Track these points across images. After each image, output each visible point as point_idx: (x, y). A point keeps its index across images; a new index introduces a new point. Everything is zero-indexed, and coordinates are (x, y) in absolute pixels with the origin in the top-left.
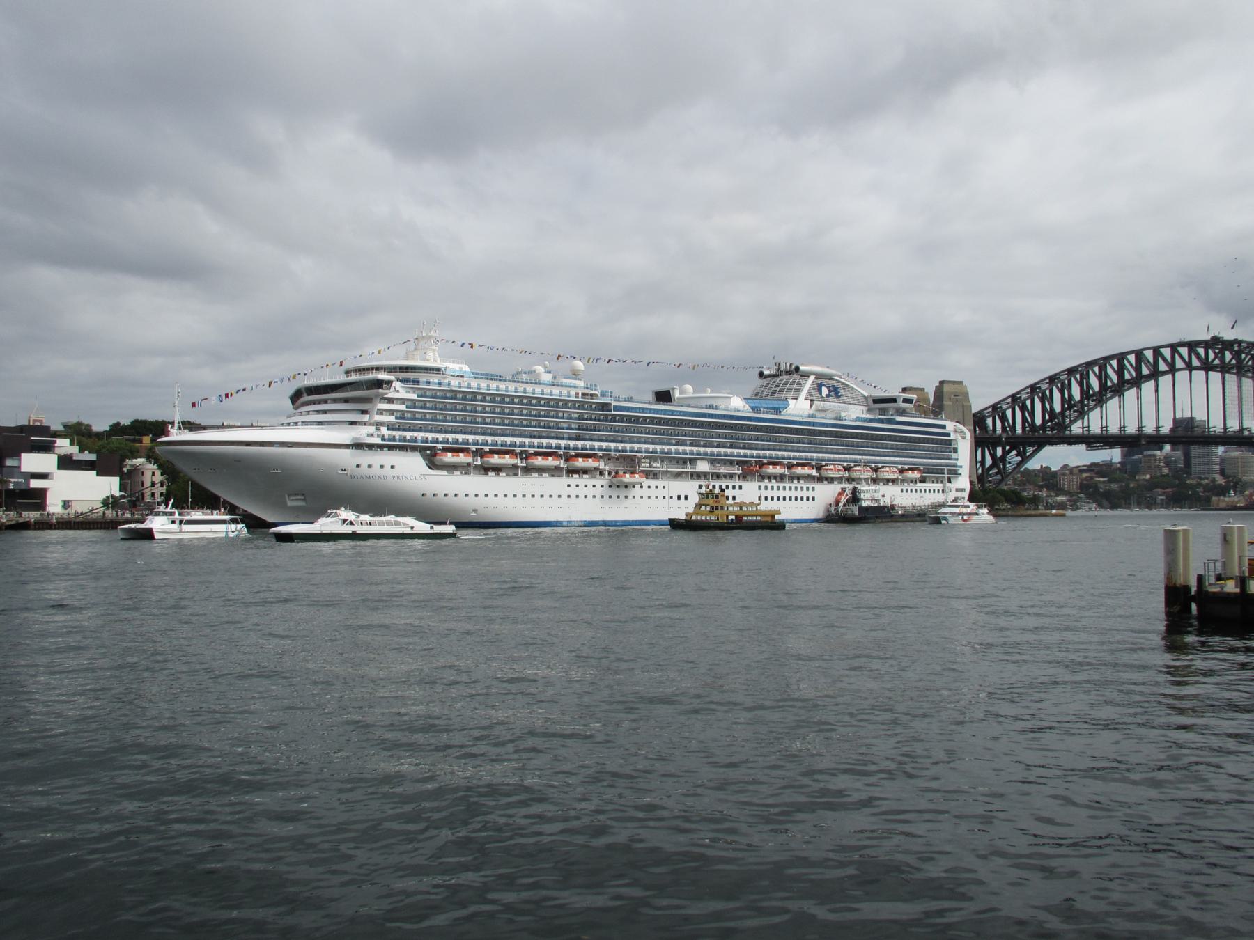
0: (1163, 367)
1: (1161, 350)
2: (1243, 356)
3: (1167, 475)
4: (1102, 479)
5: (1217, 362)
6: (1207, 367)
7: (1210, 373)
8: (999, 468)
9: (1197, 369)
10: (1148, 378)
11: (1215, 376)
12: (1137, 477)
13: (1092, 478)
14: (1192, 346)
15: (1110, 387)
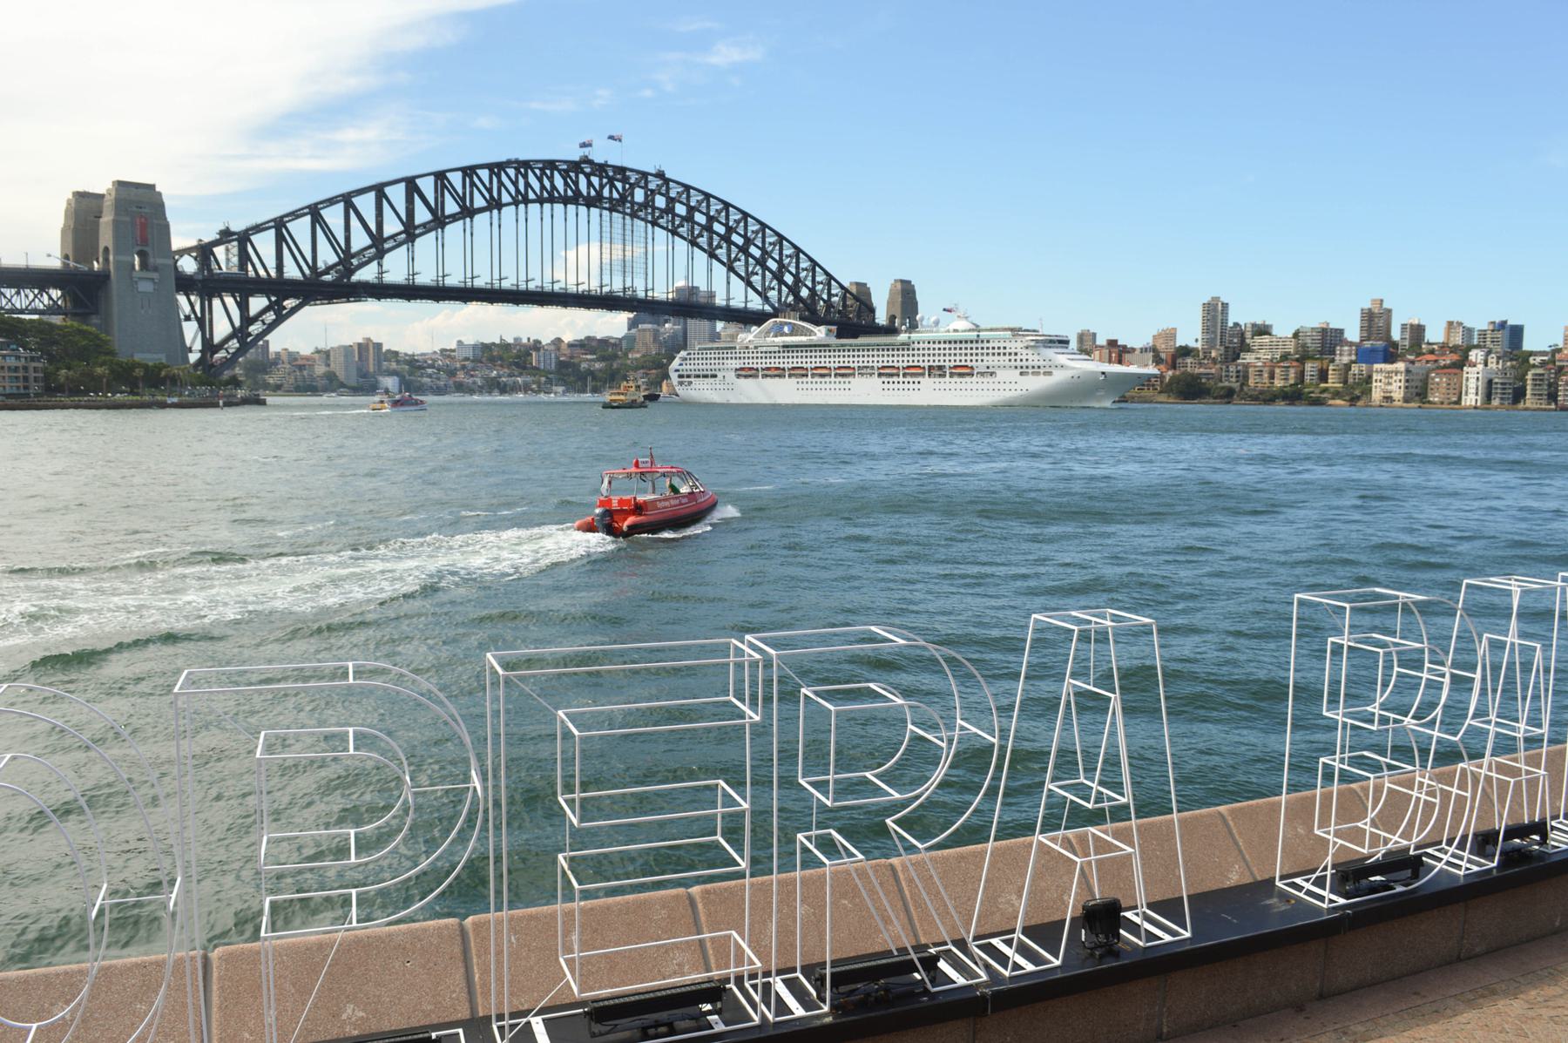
4: (589, 357)
6: (590, 203)
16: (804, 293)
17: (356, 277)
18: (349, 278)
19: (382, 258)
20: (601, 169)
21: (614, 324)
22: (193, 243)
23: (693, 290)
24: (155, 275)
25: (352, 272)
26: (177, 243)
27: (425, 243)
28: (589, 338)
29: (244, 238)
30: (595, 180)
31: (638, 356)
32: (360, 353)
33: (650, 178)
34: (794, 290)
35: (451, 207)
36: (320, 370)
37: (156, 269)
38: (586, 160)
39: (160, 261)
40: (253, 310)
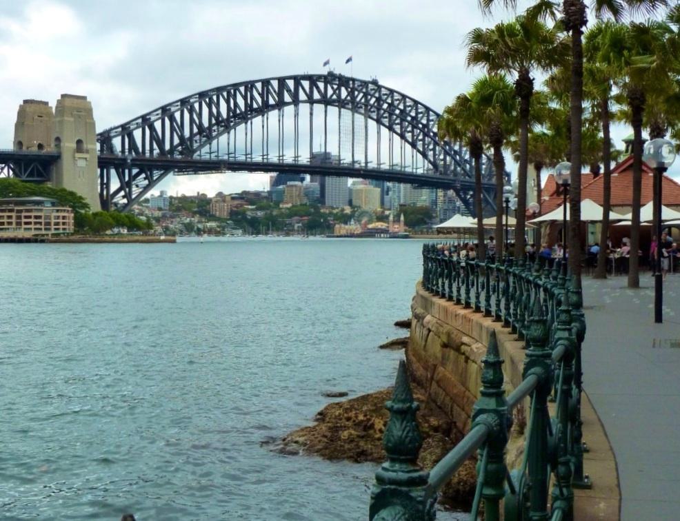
0: (287, 98)
1: (287, 81)
2: (356, 93)
3: (306, 205)
4: (250, 207)
5: (335, 97)
6: (326, 101)
7: (329, 107)
8: (125, 192)
9: (318, 102)
10: (273, 107)
11: (333, 110)
12: (281, 206)
13: (242, 205)
14: (313, 79)
15: (238, 115)
17: (196, 156)
18: (192, 157)
19: (210, 144)
21: (260, 182)
23: (326, 155)
25: (194, 151)
28: (245, 193)
29: (126, 130)
30: (335, 87)
31: (289, 205)
33: (371, 86)
37: (87, 152)
38: (331, 74)
39: (90, 146)
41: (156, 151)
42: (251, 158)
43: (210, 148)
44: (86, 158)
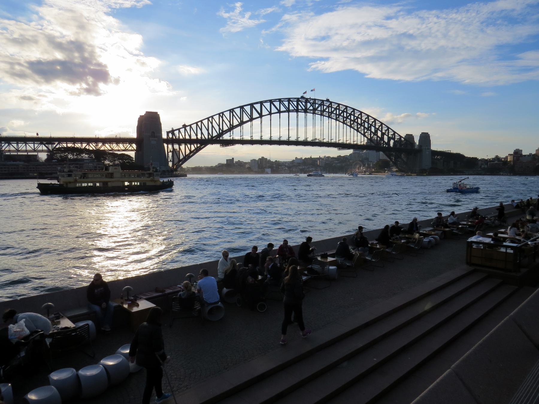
4: (337, 162)
6: (306, 111)
16: (386, 138)
18: (219, 139)
19: (230, 132)
20: (307, 100)
21: (348, 152)
22: (171, 129)
24: (156, 139)
26: (165, 128)
27: (247, 126)
32: (260, 162)
34: (382, 138)
35: (255, 115)
36: (247, 166)
40: (192, 150)
41: (210, 136)
42: (252, 138)
43: (230, 134)
44: (156, 140)
